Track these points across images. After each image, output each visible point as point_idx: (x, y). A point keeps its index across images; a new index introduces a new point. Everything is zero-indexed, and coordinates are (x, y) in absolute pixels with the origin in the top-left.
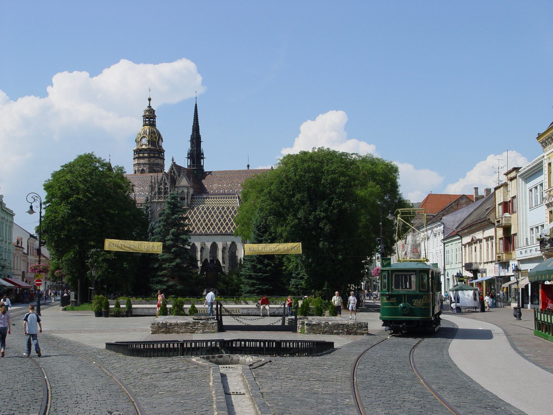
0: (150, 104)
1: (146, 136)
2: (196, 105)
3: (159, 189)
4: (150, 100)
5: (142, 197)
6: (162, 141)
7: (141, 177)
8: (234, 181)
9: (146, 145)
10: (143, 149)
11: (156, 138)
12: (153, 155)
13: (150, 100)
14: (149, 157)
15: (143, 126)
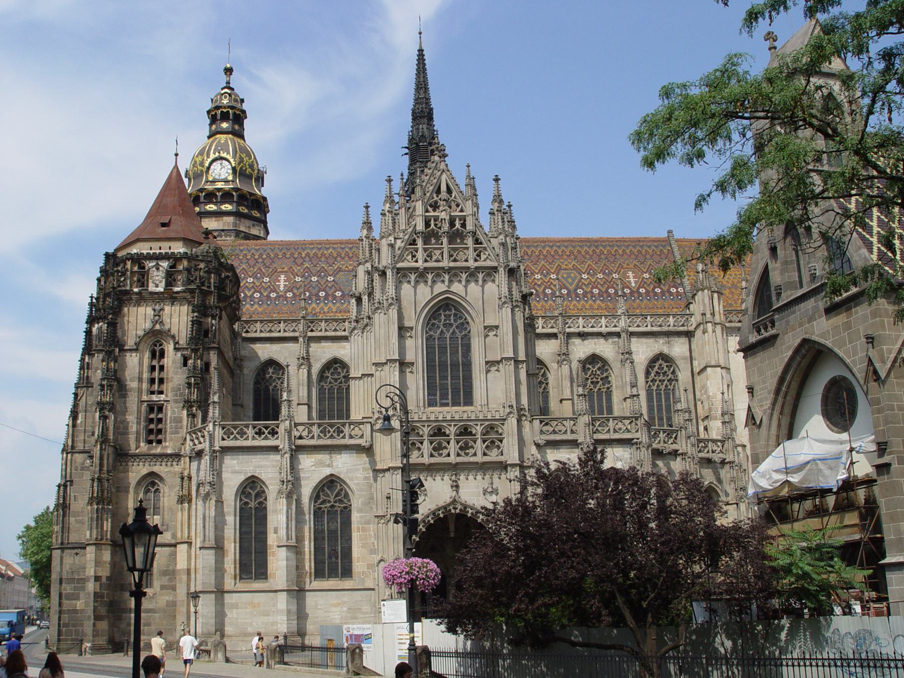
0: (228, 83)
1: (228, 157)
2: (421, 51)
3: (427, 224)
4: (229, 71)
5: (256, 306)
6: (263, 186)
7: (241, 251)
8: (563, 267)
9: (226, 181)
10: (219, 190)
11: (251, 166)
12: (246, 211)
13: (229, 71)
14: (237, 214)
15: (209, 137)
